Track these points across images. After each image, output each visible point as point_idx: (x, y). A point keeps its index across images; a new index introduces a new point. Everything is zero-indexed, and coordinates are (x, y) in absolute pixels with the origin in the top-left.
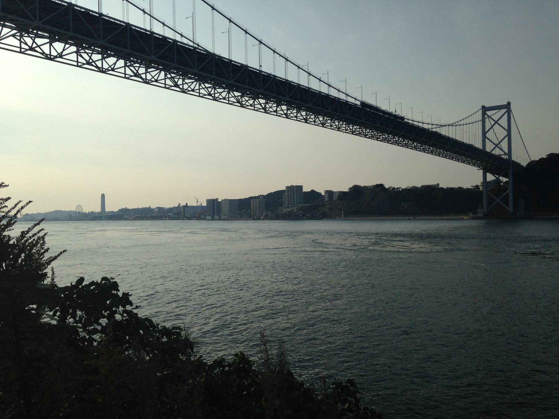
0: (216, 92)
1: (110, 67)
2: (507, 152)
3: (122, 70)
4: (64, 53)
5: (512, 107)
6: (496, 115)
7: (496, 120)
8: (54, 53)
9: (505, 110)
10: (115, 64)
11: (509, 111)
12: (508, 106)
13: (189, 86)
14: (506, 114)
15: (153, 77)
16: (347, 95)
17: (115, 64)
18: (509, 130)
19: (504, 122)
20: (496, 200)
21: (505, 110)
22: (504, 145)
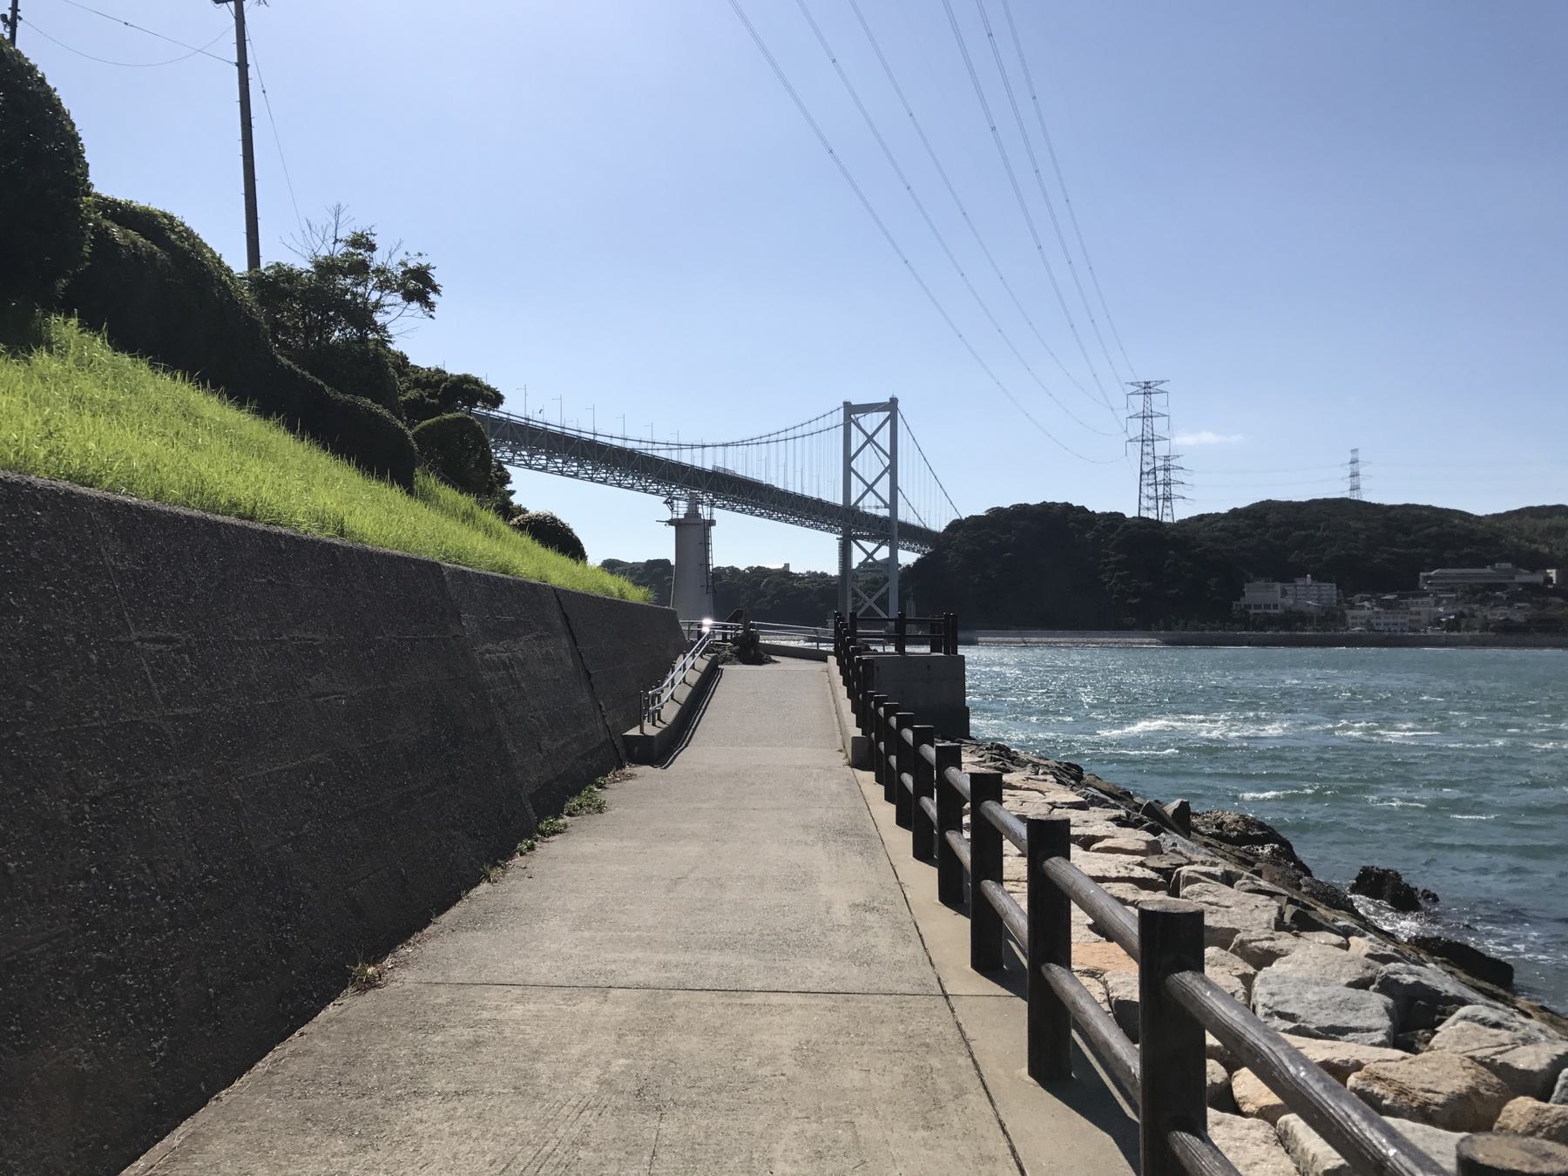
6: (870, 421)
9: (888, 413)
11: (893, 419)
12: (892, 406)
14: (888, 424)
18: (893, 456)
19: (883, 439)
21: (888, 413)
22: (883, 488)
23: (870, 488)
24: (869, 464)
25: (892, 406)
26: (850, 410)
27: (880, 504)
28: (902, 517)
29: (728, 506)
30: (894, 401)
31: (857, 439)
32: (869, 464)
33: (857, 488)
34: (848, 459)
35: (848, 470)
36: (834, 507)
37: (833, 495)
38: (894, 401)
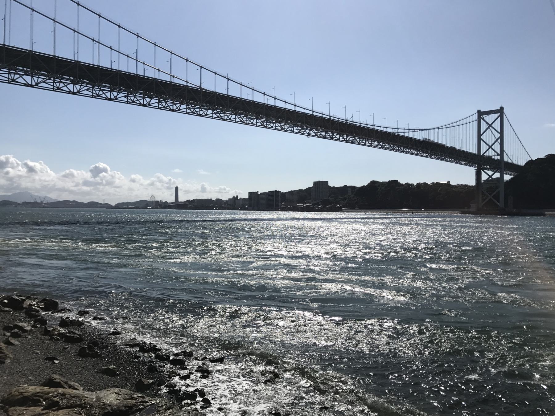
0: (236, 117)
1: (148, 103)
2: (499, 153)
3: (157, 105)
4: (118, 97)
5: (505, 111)
6: (490, 118)
7: (490, 123)
8: (112, 97)
9: (499, 114)
10: (150, 101)
11: (501, 117)
12: (501, 111)
13: (204, 112)
15: (177, 108)
16: (295, 106)
17: (150, 101)
18: (501, 133)
19: (497, 125)
20: (490, 199)
21: (499, 114)
22: (497, 147)
23: (490, 147)
24: (489, 137)
25: (501, 111)
26: (480, 114)
27: (496, 154)
28: (506, 159)
29: (420, 154)
30: (502, 109)
31: (484, 126)
32: (489, 137)
33: (484, 147)
34: (480, 135)
35: (480, 140)
36: (472, 154)
37: (474, 150)
38: (502, 109)
